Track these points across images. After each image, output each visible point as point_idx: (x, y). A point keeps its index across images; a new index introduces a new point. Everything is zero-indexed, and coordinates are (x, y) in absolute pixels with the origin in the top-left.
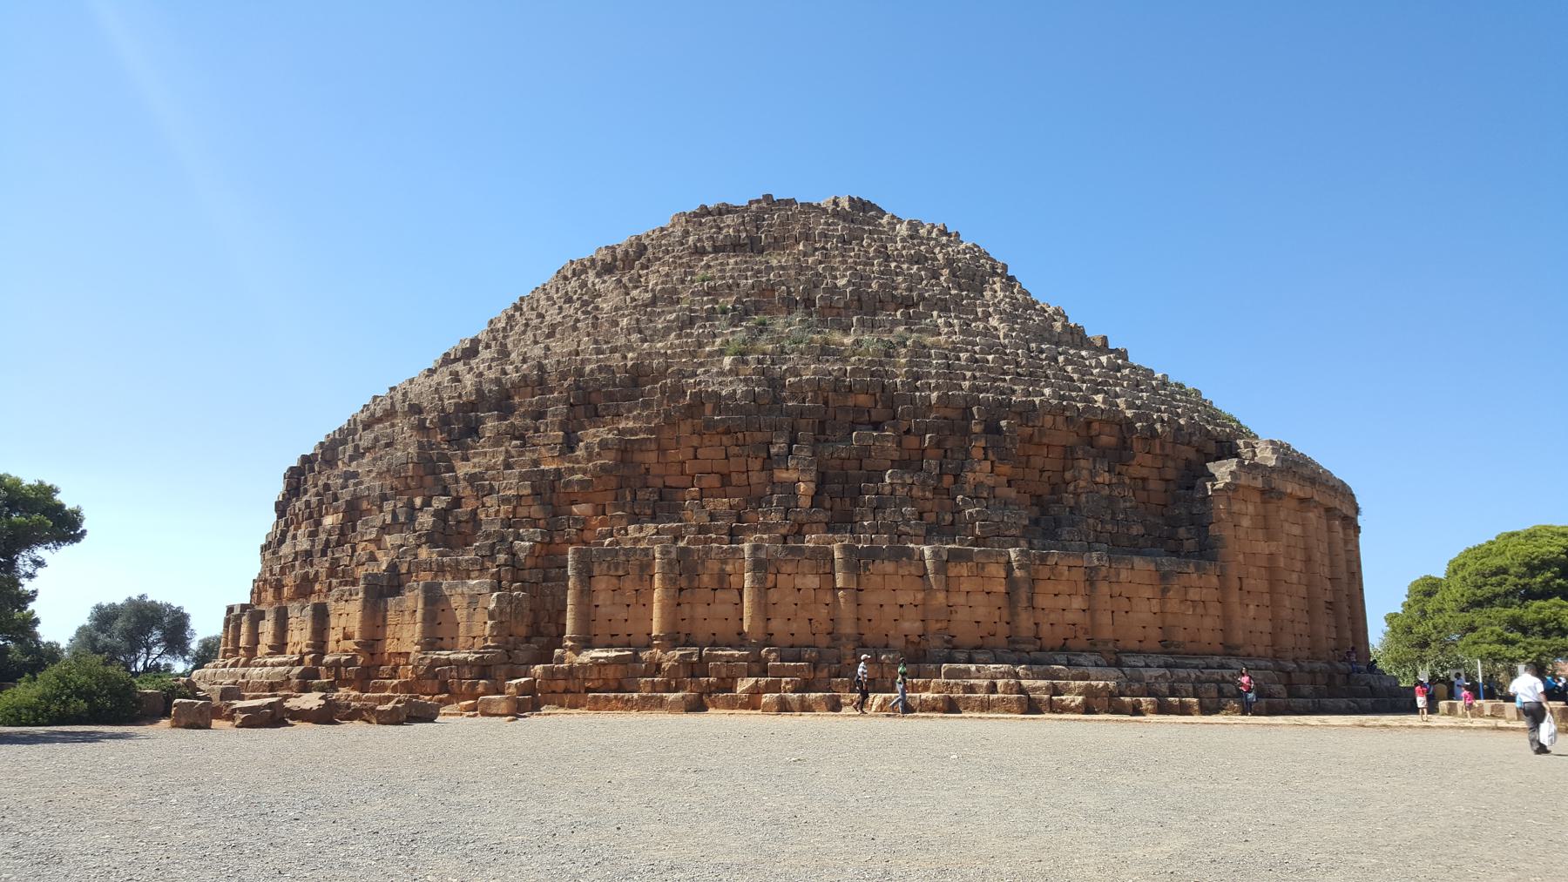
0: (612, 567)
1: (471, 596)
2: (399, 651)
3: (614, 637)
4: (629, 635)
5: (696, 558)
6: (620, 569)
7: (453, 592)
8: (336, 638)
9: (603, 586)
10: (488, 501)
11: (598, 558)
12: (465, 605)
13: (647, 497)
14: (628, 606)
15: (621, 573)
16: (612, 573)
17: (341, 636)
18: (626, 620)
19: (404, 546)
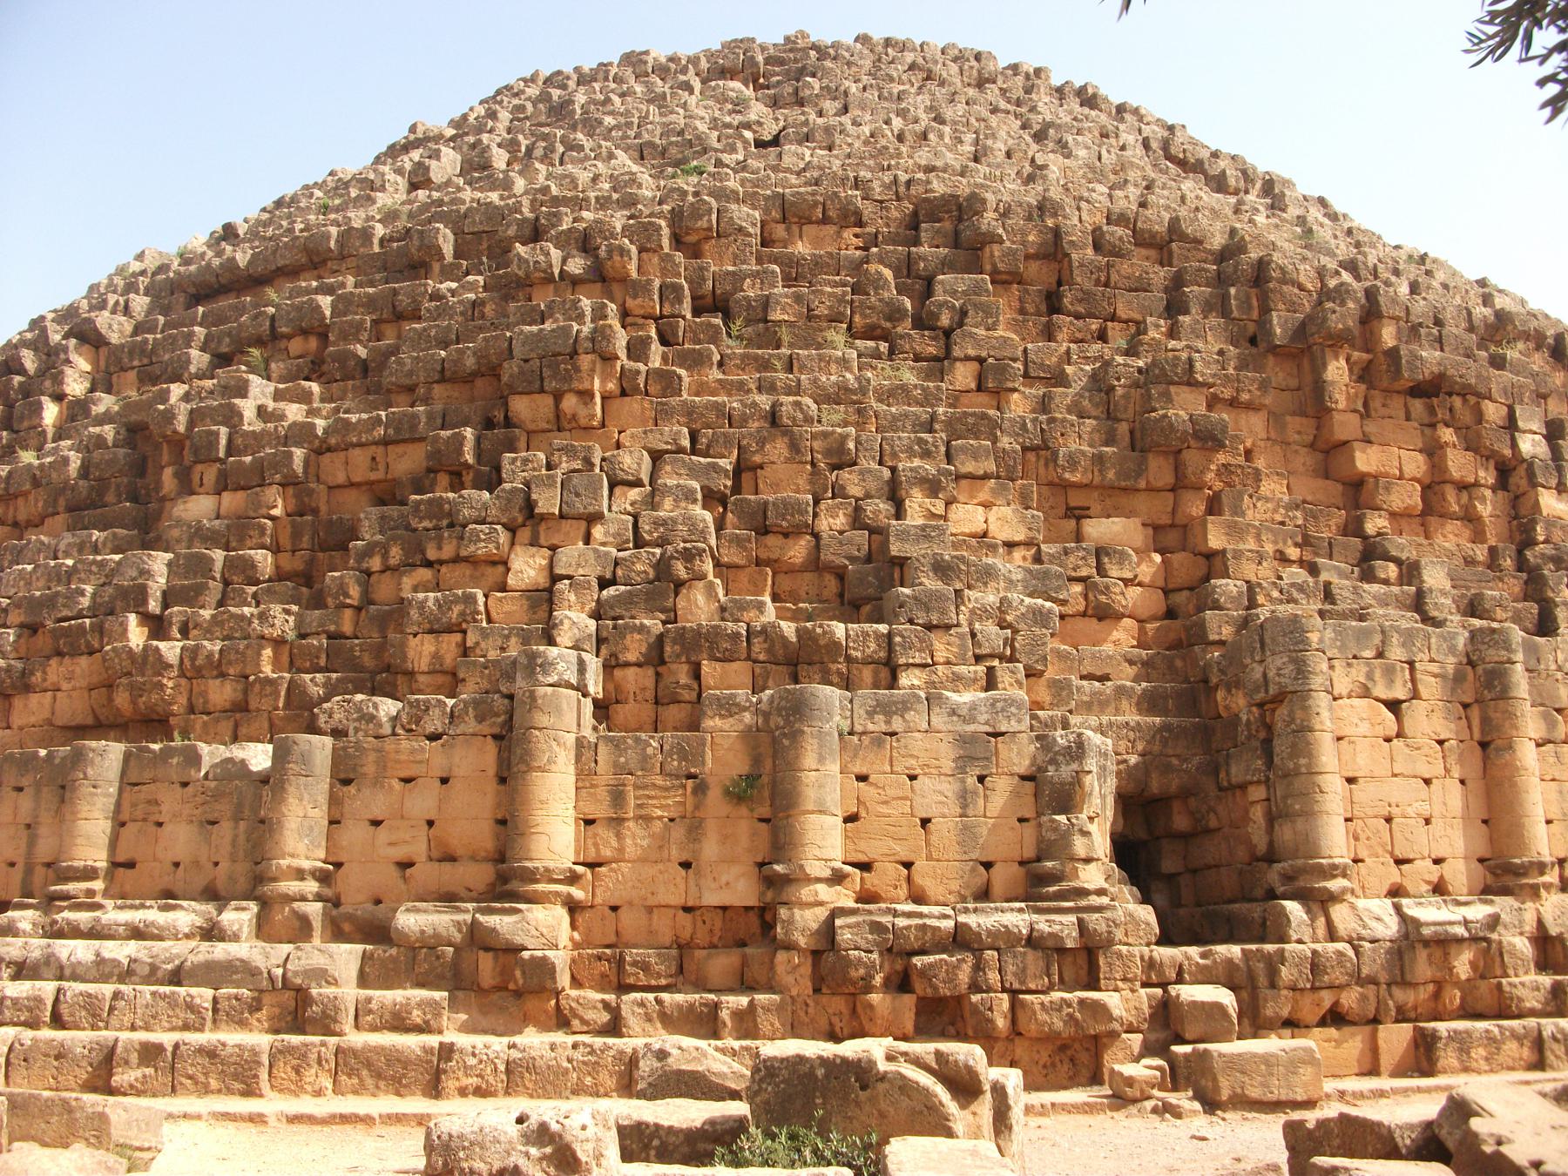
0: (1378, 675)
1: (963, 740)
2: (690, 904)
3: (1405, 867)
4: (1437, 861)
5: (1553, 667)
6: (1399, 683)
7: (897, 724)
8: (400, 853)
9: (1364, 728)
10: (852, 482)
11: (1340, 649)
12: (948, 765)
13: (1279, 518)
14: (1427, 782)
15: (1400, 692)
16: (1380, 691)
17: (418, 849)
18: (1428, 821)
19: (613, 582)
